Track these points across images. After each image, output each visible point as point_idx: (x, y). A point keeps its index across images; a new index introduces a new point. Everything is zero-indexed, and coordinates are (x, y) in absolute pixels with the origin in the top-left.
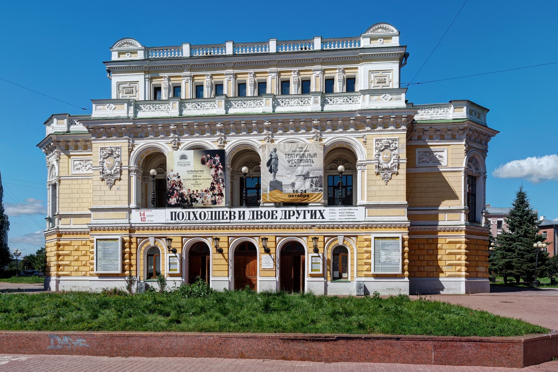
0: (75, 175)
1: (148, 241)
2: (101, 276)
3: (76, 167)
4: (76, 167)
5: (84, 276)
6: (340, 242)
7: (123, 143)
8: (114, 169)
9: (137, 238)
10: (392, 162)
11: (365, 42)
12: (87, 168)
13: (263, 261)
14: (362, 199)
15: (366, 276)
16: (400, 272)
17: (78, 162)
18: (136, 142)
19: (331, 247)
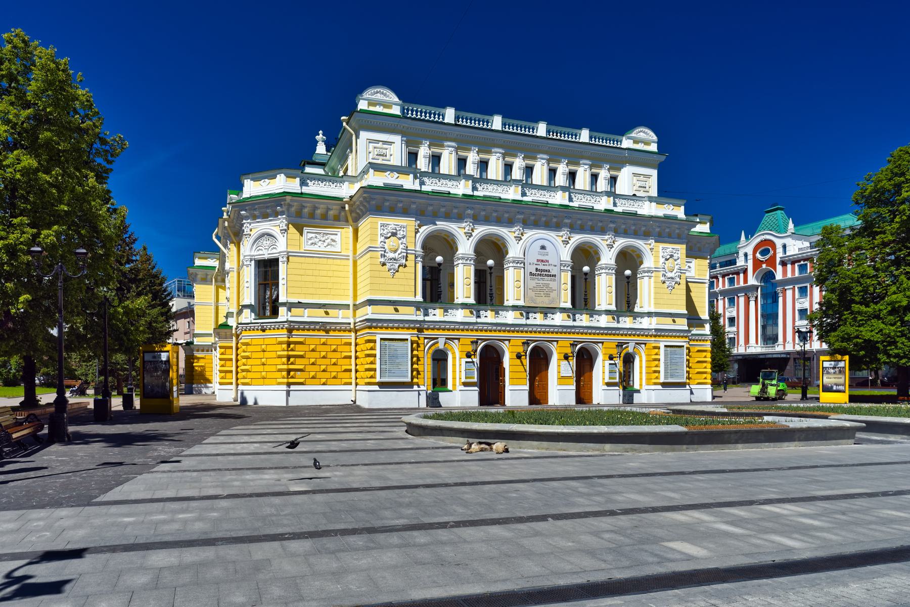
0: (311, 252)
1: (437, 343)
2: (382, 385)
3: (310, 242)
4: (310, 242)
5: (324, 384)
6: (441, 346)
7: (409, 223)
8: (399, 252)
9: (425, 338)
10: (399, 252)
11: (626, 143)
12: (325, 244)
13: (562, 368)
14: (649, 306)
15: (655, 384)
16: (409, 380)
17: (313, 235)
18: (476, 227)
19: (431, 351)
